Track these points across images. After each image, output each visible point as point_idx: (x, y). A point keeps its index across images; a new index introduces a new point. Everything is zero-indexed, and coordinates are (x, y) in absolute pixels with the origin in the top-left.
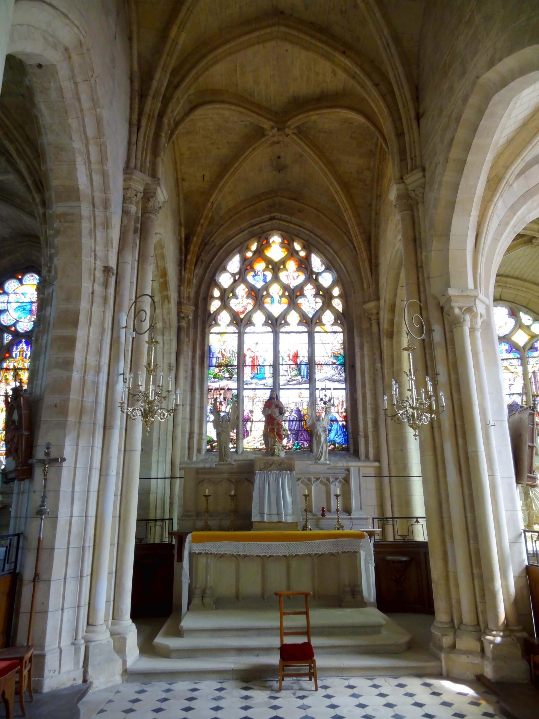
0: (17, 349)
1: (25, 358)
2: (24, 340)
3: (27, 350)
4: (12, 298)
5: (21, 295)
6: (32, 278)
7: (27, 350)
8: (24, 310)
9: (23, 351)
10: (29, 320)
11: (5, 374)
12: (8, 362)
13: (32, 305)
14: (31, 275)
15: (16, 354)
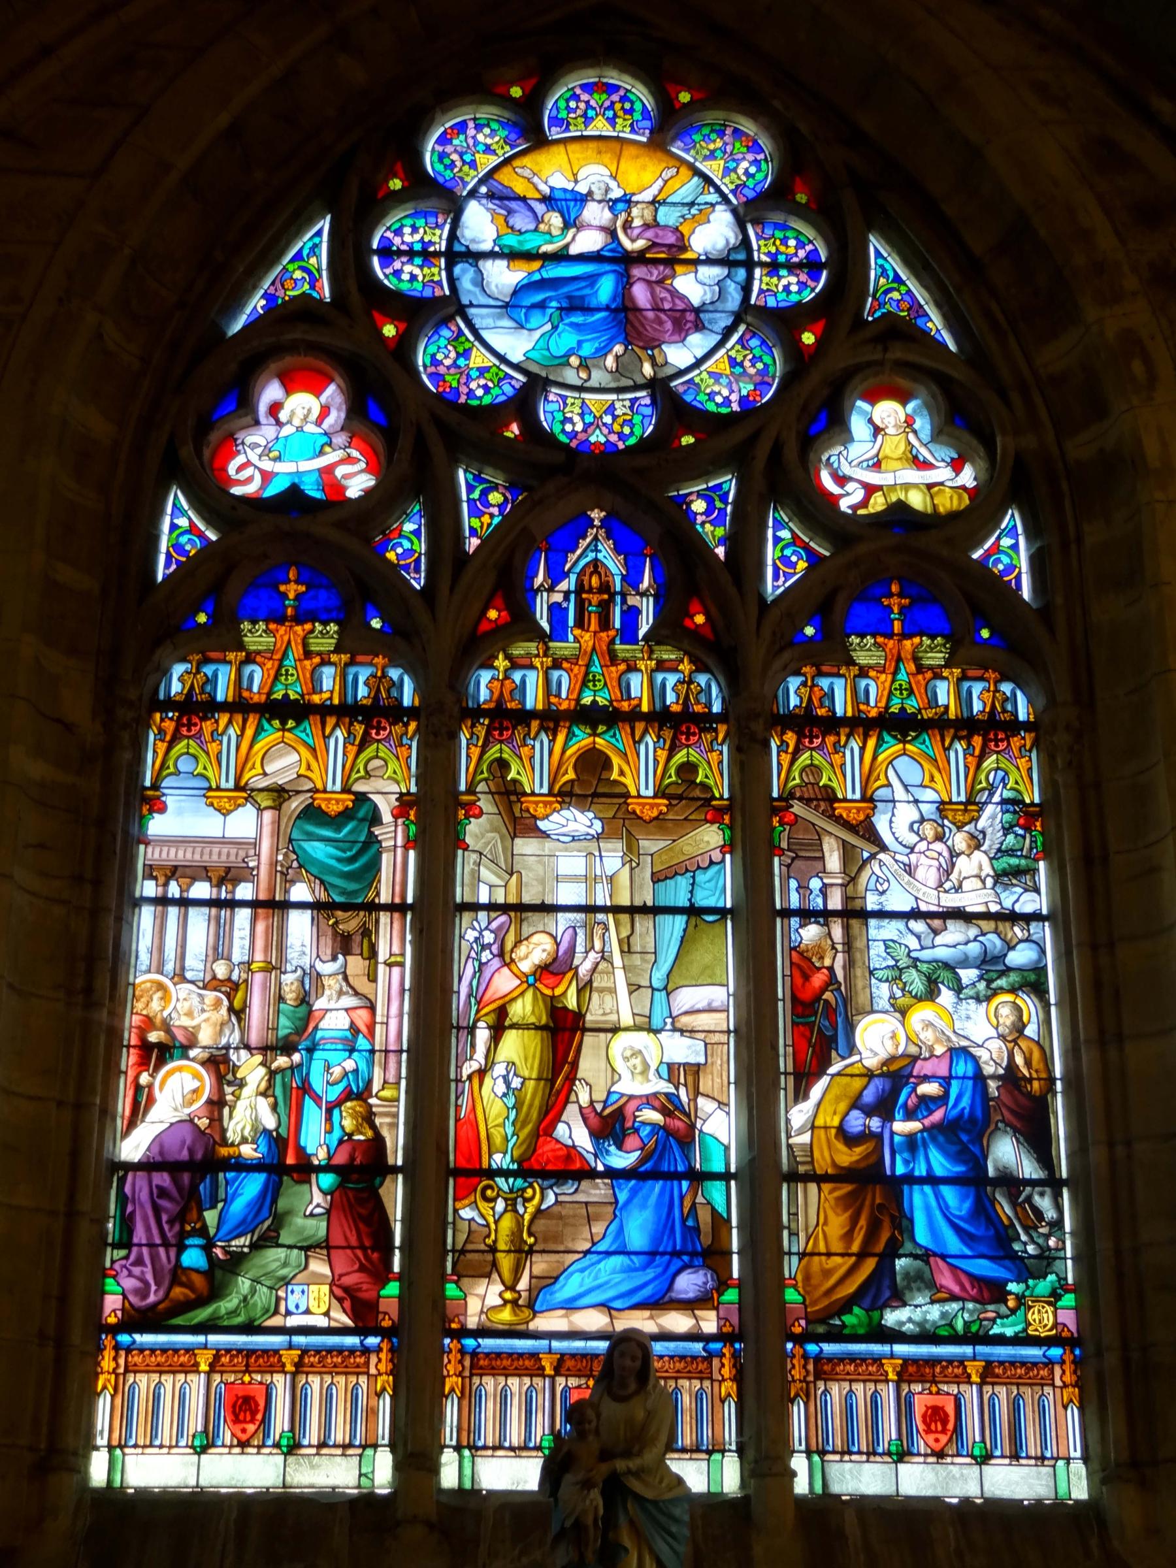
0: (556, 575)
1: (629, 633)
2: (596, 515)
3: (632, 579)
4: (479, 224)
5: (540, 208)
6: (598, 99)
7: (632, 579)
8: (575, 305)
9: (605, 587)
10: (618, 372)
11: (493, 752)
12: (501, 663)
13: (625, 283)
14: (590, 76)
15: (554, 608)
